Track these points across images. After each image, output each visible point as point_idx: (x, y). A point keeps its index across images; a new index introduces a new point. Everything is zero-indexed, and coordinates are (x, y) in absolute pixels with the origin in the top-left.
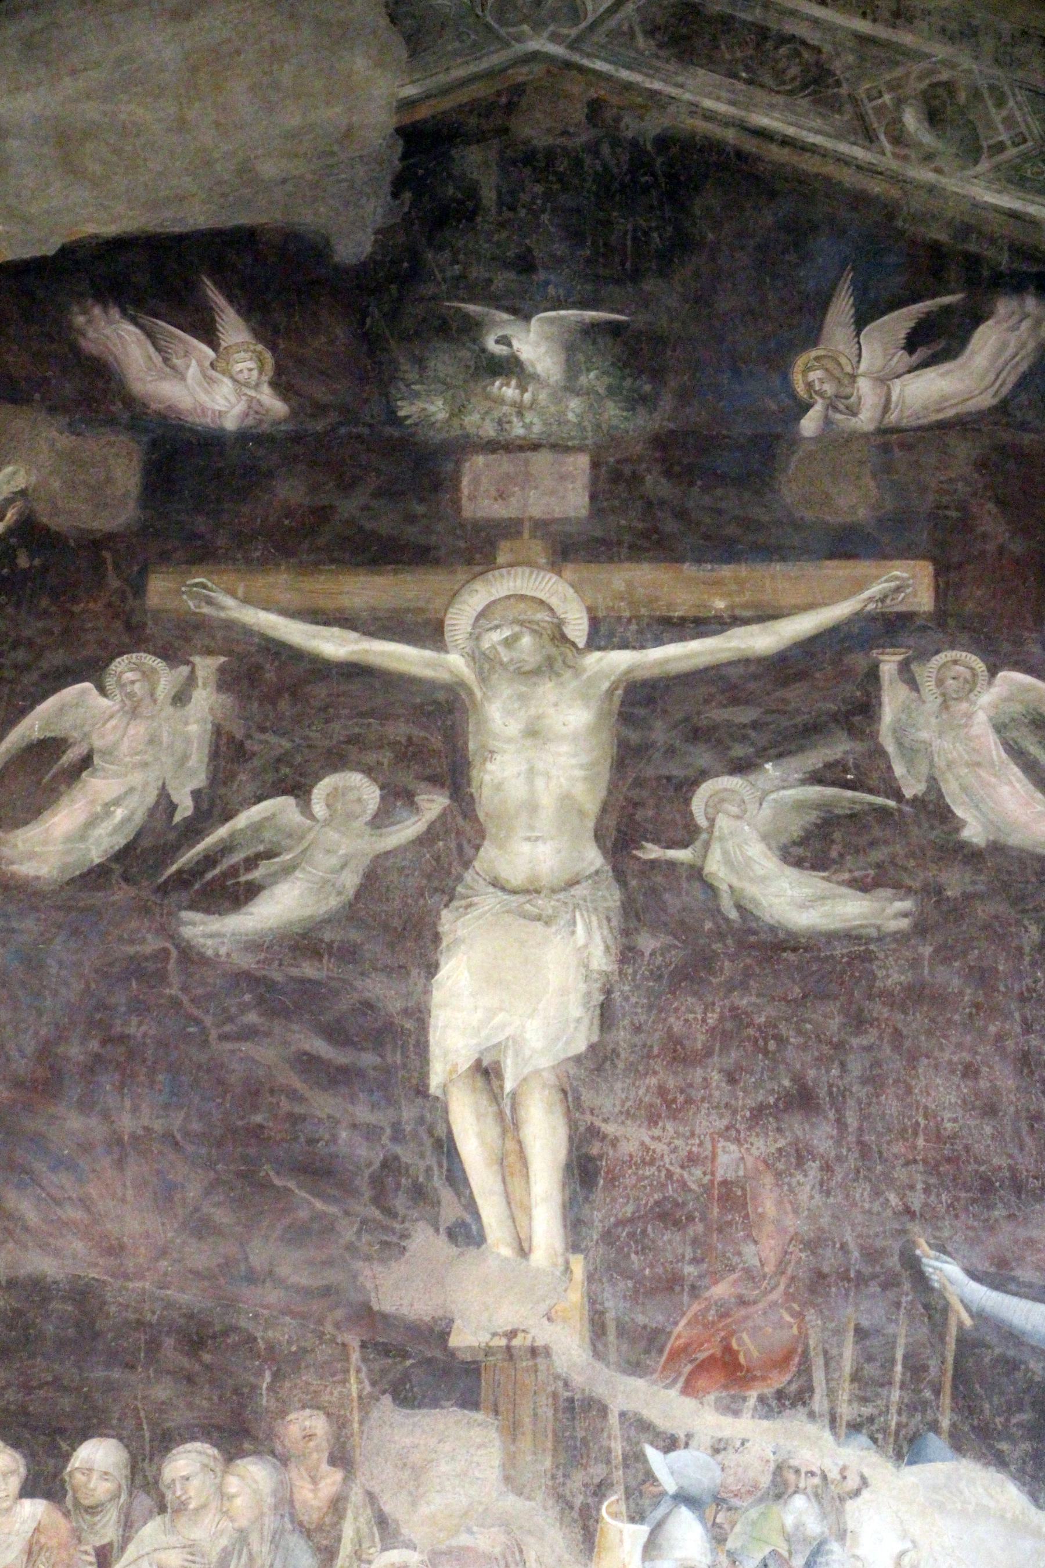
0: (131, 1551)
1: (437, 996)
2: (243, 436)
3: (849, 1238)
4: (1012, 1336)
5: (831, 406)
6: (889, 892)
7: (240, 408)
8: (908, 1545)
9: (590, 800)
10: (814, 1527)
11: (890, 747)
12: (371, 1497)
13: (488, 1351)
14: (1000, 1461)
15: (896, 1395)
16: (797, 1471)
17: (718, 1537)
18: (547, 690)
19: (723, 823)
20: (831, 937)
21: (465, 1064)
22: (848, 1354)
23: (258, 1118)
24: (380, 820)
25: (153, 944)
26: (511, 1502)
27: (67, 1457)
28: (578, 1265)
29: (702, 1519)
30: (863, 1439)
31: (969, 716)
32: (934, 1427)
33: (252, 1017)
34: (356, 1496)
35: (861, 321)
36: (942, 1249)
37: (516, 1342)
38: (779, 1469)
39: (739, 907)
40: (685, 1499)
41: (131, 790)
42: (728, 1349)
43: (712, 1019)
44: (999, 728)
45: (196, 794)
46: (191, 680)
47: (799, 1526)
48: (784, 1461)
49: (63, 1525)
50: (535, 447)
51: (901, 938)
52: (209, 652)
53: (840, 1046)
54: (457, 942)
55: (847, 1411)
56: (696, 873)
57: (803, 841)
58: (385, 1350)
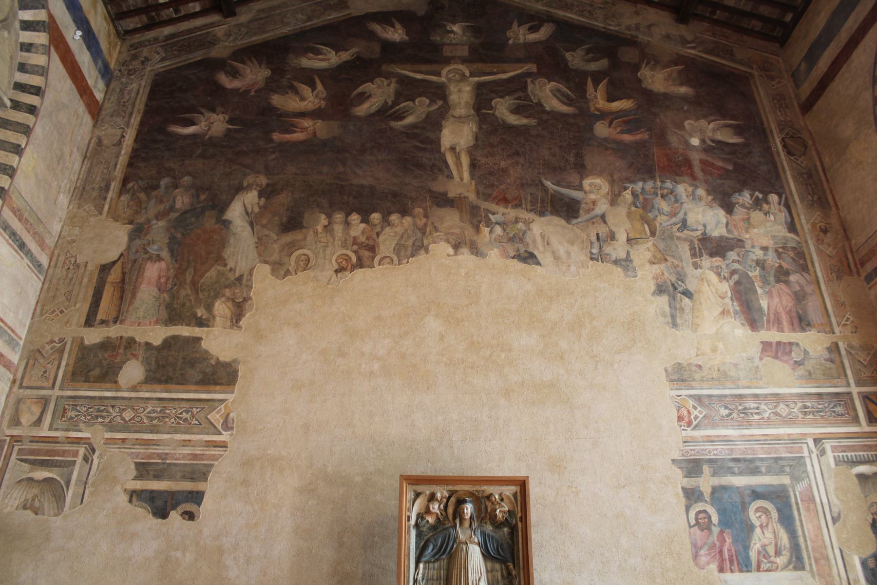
0: (383, 233)
1: (442, 135)
2: (400, 43)
3: (528, 177)
4: (562, 194)
5: (515, 38)
6: (532, 119)
7: (400, 38)
9: (472, 103)
10: (524, 228)
11: (530, 94)
12: (433, 223)
13: (455, 197)
14: (560, 216)
15: (539, 205)
17: (504, 230)
18: (462, 84)
19: (498, 106)
20: (521, 126)
21: (448, 147)
22: (529, 197)
23: (407, 157)
24: (429, 105)
25: (384, 126)
26: (461, 224)
27: (370, 216)
28: (473, 182)
29: (501, 227)
30: (533, 213)
31: (545, 89)
32: (547, 210)
33: (405, 139)
34: (429, 223)
35: (519, 26)
36: (547, 179)
38: (516, 218)
39: (502, 121)
40: (497, 223)
41: (379, 100)
42: (505, 197)
43: (498, 140)
44: (551, 91)
45: (392, 101)
46: (391, 82)
47: (521, 228)
49: (369, 228)
50: (457, 45)
51: (534, 126)
52: (394, 77)
53: (524, 144)
54: (446, 126)
55: (529, 208)
56: (493, 115)
57: (515, 109)
58: (434, 197)
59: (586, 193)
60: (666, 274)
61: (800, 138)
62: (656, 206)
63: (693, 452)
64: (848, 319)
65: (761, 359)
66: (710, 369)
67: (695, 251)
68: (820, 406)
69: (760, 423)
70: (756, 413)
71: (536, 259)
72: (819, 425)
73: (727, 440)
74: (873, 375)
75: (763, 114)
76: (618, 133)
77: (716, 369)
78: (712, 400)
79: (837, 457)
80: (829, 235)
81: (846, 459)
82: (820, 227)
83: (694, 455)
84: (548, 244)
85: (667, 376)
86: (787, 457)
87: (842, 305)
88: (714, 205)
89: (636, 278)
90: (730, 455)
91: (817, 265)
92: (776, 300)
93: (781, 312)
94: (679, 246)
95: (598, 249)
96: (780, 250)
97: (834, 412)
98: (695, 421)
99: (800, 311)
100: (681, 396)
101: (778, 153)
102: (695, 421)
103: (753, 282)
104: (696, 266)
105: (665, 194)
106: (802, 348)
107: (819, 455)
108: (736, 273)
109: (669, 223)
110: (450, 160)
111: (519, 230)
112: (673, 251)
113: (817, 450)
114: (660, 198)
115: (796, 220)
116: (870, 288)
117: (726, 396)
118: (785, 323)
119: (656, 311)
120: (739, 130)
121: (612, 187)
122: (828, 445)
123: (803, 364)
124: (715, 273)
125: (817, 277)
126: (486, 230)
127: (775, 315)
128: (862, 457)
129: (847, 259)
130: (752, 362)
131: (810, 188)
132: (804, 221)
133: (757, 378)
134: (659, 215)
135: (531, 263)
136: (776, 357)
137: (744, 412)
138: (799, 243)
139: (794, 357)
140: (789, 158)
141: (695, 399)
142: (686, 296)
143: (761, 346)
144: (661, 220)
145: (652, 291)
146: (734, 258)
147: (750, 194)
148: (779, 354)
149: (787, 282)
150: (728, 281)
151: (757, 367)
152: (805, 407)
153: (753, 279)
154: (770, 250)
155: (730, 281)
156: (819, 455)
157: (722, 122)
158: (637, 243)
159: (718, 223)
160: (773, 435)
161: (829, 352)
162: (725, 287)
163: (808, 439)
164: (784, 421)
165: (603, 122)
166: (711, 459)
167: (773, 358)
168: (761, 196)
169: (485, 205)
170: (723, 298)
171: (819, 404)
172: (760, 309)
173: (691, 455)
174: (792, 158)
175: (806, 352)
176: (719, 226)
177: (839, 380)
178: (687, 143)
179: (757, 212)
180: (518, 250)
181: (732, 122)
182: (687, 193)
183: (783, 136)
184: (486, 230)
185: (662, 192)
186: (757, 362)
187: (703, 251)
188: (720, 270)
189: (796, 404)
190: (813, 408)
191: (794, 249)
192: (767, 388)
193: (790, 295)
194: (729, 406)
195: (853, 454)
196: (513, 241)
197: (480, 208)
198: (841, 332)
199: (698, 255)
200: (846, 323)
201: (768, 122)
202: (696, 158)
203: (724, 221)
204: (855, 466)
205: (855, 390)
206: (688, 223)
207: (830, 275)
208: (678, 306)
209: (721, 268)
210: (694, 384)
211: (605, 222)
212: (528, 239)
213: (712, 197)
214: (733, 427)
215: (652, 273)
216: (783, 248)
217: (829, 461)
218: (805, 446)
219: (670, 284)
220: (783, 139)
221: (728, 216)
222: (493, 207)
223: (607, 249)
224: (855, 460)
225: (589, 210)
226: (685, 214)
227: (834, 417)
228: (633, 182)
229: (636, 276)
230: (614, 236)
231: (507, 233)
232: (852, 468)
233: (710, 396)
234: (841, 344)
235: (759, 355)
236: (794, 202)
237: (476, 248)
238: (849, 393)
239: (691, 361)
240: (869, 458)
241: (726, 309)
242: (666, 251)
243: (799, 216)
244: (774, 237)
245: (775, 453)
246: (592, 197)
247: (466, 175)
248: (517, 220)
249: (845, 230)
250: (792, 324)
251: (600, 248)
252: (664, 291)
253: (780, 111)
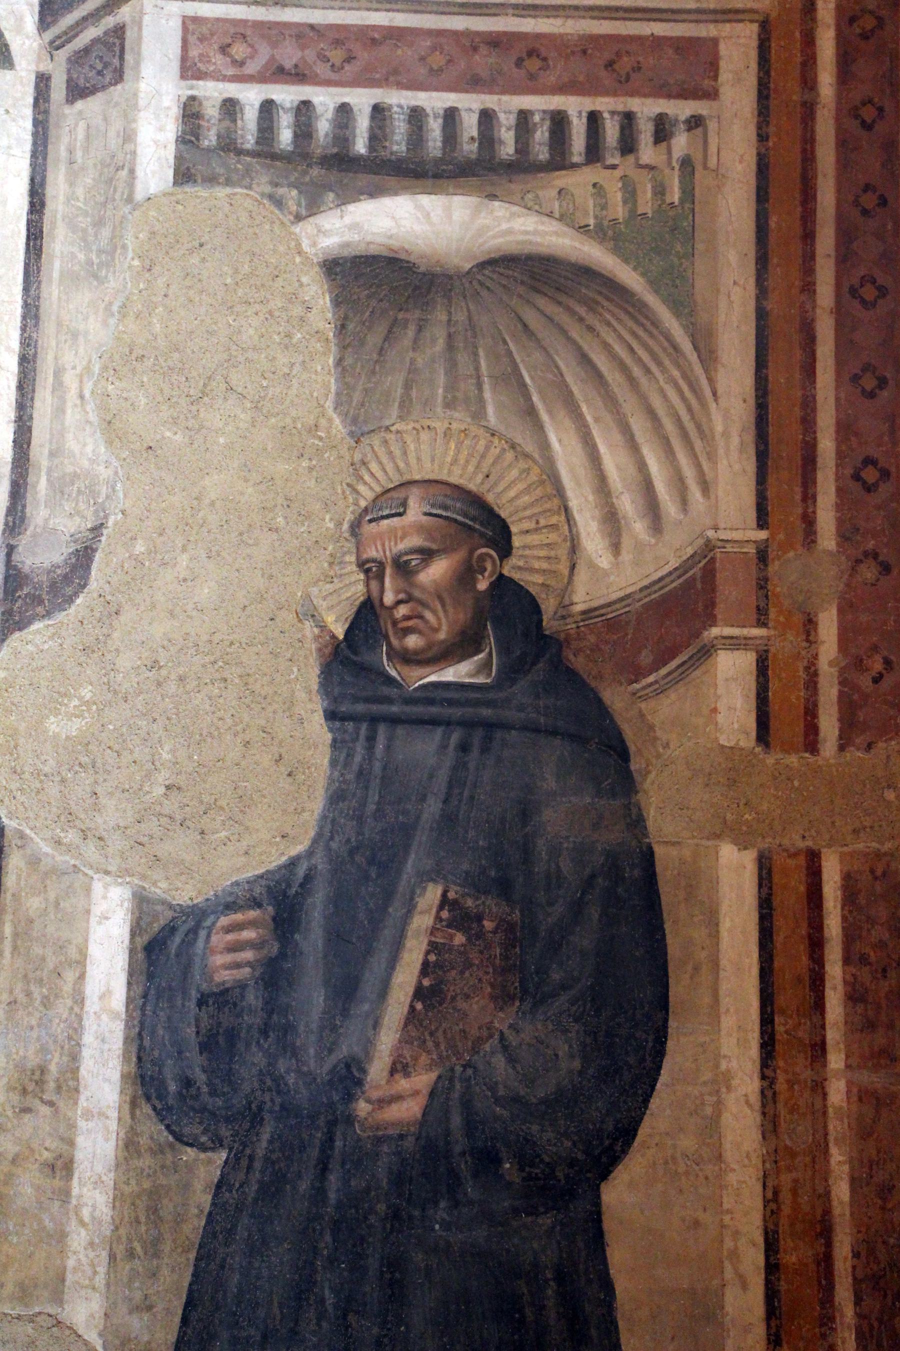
79: (212, 111)
81: (285, 136)
113: (55, 46)
128: (435, 128)
204: (347, 197)
217: (129, 137)
224: (361, 146)
232: (313, 207)
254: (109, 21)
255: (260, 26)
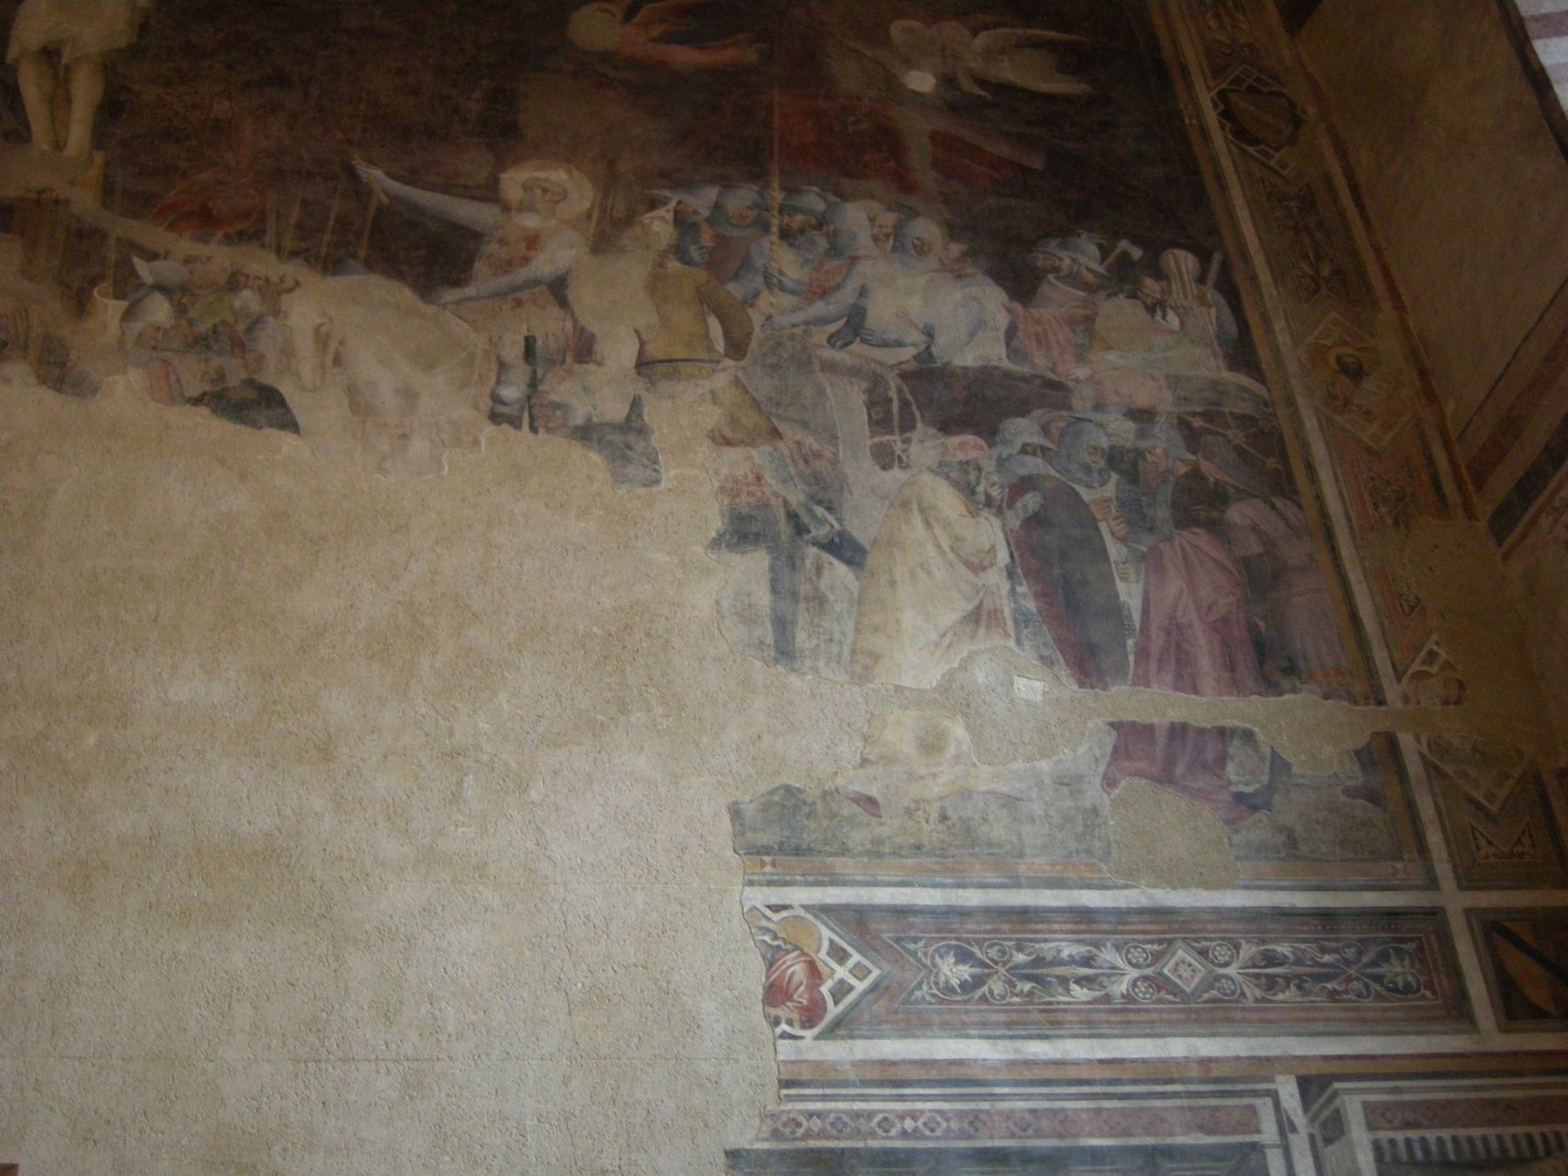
8: (326, 320)
14: (400, 276)
16: (247, 276)
17: (180, 310)
22: (295, 214)
28: (99, 158)
29: (171, 300)
32: (354, 256)
36: (371, 162)
37: (43, 196)
38: (234, 275)
48: (238, 270)
55: (288, 244)
59: (507, 209)
60: (769, 478)
61: (1281, 95)
62: (759, 263)
63: (816, 1124)
64: (1432, 656)
65: (1109, 782)
66: (909, 812)
67: (889, 412)
68: (1327, 958)
69: (1095, 1017)
70: (1081, 981)
71: (282, 411)
72: (1321, 1027)
73: (956, 1077)
74: (1519, 849)
75: (1158, 20)
76: (654, 40)
77: (934, 815)
78: (911, 926)
79: (1385, 1145)
80: (1368, 384)
82: (1339, 360)
83: (819, 1136)
84: (337, 361)
85: (738, 833)
86: (1193, 1148)
87: (1412, 609)
88: (970, 271)
89: (655, 489)
90: (969, 1137)
91: (1325, 475)
92: (1175, 585)
93: (1190, 625)
94: (829, 392)
95: (523, 387)
96: (1197, 423)
97: (1378, 979)
98: (836, 1003)
99: (1261, 624)
100: (785, 907)
101: (1204, 133)
102: (836, 1003)
103: (1095, 522)
104: (885, 459)
105: (795, 226)
106: (1266, 751)
107: (1319, 1138)
108: (1035, 489)
109: (801, 316)
110: (32, 87)
111: (235, 313)
112: (804, 407)
113: (1313, 1120)
114: (775, 238)
115: (1257, 333)
116: (1506, 557)
117: (964, 913)
118: (1205, 661)
119: (717, 602)
120: (1072, 60)
121: (606, 196)
122: (1353, 1105)
123: (1268, 805)
124: (955, 484)
125: (1324, 515)
126: (110, 309)
127: (1168, 633)
128: (1479, 1144)
129: (1431, 461)
130: (1076, 794)
131: (1307, 240)
132: (1283, 339)
133: (1089, 852)
134: (765, 294)
135: (263, 420)
136: (1166, 778)
137: (1038, 972)
138: (1266, 404)
139: (1234, 778)
140: (1240, 149)
141: (843, 923)
142: (840, 558)
143: (1110, 740)
144: (772, 304)
145: (713, 534)
146: (1028, 439)
147: (1100, 247)
148: (1180, 769)
149: (1217, 528)
150: (1000, 512)
151: (1095, 811)
152: (1271, 959)
153: (1093, 508)
154: (1161, 419)
155: (1008, 513)
156: (1320, 1142)
157: (1020, 32)
158: (674, 375)
159: (980, 325)
160: (1144, 1061)
161: (1363, 765)
162: (989, 534)
163: (1279, 1078)
164: (1190, 1010)
165: (605, 6)
166: (888, 1152)
167: (1158, 781)
168: (1136, 253)
169: (123, 227)
170: (978, 568)
171: (1323, 950)
172: (1115, 611)
173: (808, 1135)
174: (1250, 149)
175: (1279, 765)
176: (980, 334)
177: (1399, 865)
178: (894, 90)
179: (1122, 300)
180: (221, 376)
181: (1053, 34)
182: (876, 230)
183: (1224, 86)
184: (110, 309)
185: (786, 219)
186: (1094, 793)
187: (917, 414)
188: (972, 476)
189: (1237, 947)
190: (1299, 962)
191: (1244, 420)
192: (1126, 887)
193: (1224, 568)
194: (976, 950)
195: (1446, 1134)
196: (208, 347)
197: (104, 236)
198: (1406, 699)
199: (896, 423)
200: (1426, 668)
201: (1175, 42)
202: (917, 128)
203: (1003, 321)
205: (1455, 901)
206: (871, 321)
207: (1370, 510)
208: (804, 589)
209: (979, 469)
210: (841, 865)
211: (563, 303)
212: (267, 343)
213: (963, 247)
214: (987, 1030)
215: (716, 473)
216: (1207, 416)
217: (1354, 1160)
218: (1265, 1107)
219: (781, 514)
220: (1222, 95)
221: (1018, 307)
222: (152, 234)
223: (559, 389)
224: (1452, 1156)
225: (509, 263)
226: (863, 292)
227: (1379, 997)
228: (689, 185)
229: (657, 482)
230: (592, 347)
231: (191, 323)
233: (901, 913)
234: (1405, 740)
235: (1102, 768)
236: (1254, 278)
237: (63, 365)
238: (1435, 914)
239: (840, 781)
240: (1503, 1149)
241: (988, 604)
242: (778, 404)
243: (1267, 322)
244: (1175, 381)
245: (1147, 1132)
246: (530, 222)
247: (78, 133)
248: (235, 282)
249: (1423, 373)
250: (1232, 668)
251: (533, 384)
252: (758, 535)
253: (1216, 16)
254: (1332, 1107)
255: (1393, 1103)
